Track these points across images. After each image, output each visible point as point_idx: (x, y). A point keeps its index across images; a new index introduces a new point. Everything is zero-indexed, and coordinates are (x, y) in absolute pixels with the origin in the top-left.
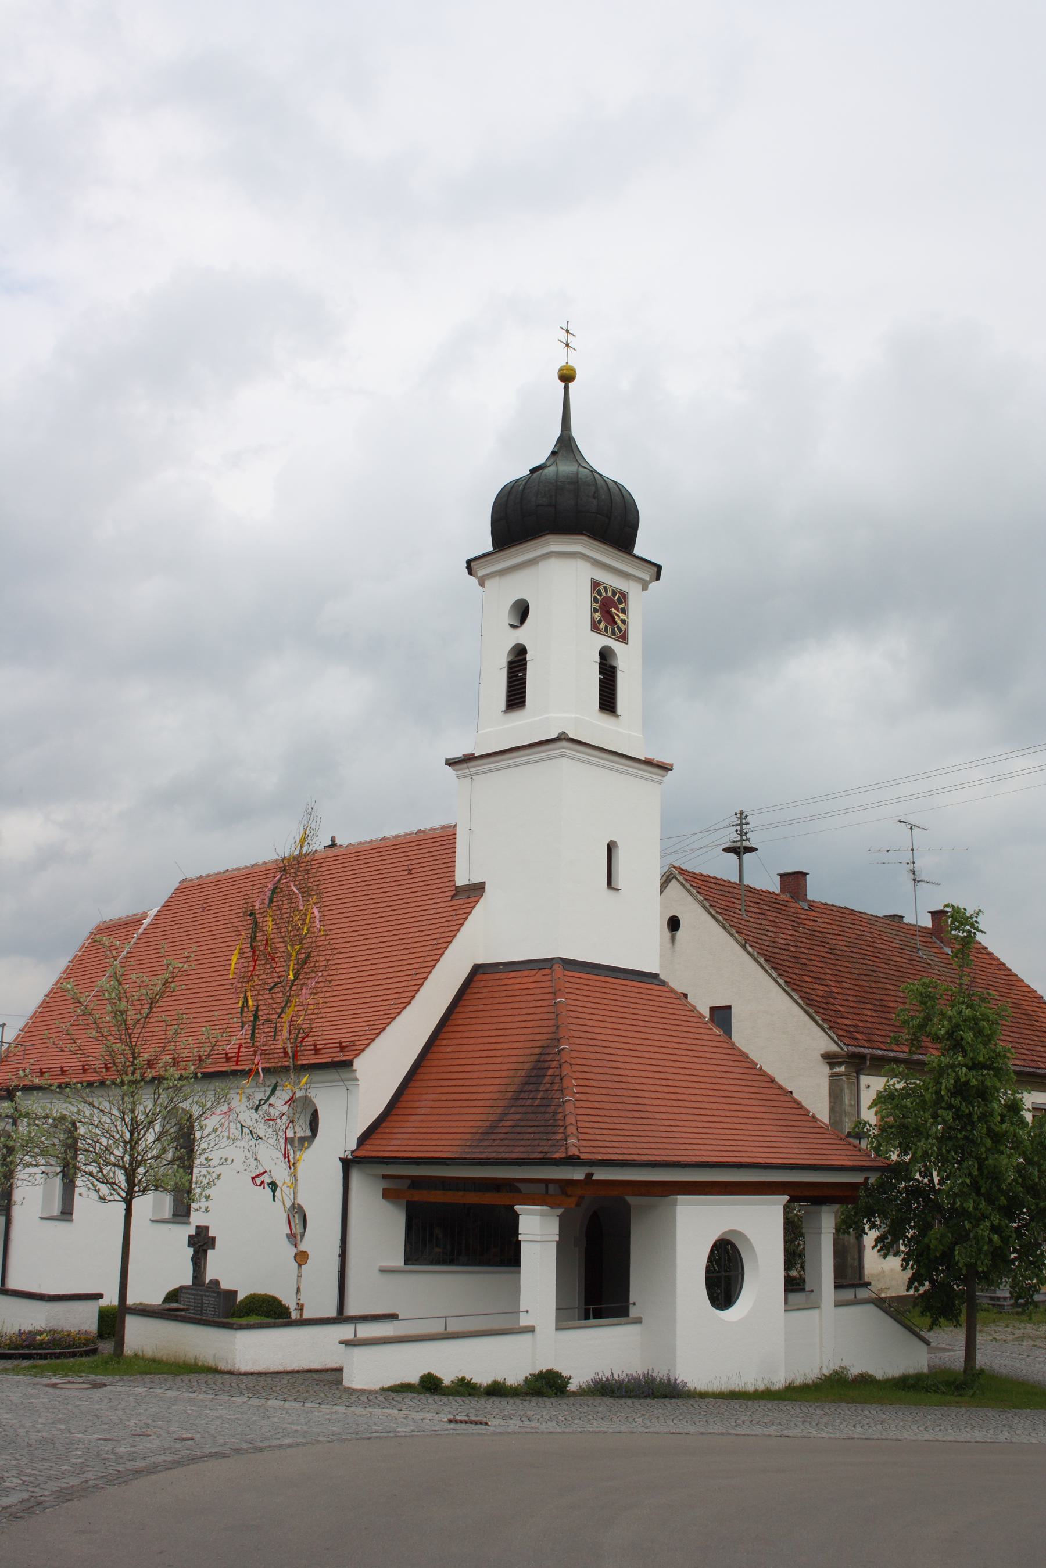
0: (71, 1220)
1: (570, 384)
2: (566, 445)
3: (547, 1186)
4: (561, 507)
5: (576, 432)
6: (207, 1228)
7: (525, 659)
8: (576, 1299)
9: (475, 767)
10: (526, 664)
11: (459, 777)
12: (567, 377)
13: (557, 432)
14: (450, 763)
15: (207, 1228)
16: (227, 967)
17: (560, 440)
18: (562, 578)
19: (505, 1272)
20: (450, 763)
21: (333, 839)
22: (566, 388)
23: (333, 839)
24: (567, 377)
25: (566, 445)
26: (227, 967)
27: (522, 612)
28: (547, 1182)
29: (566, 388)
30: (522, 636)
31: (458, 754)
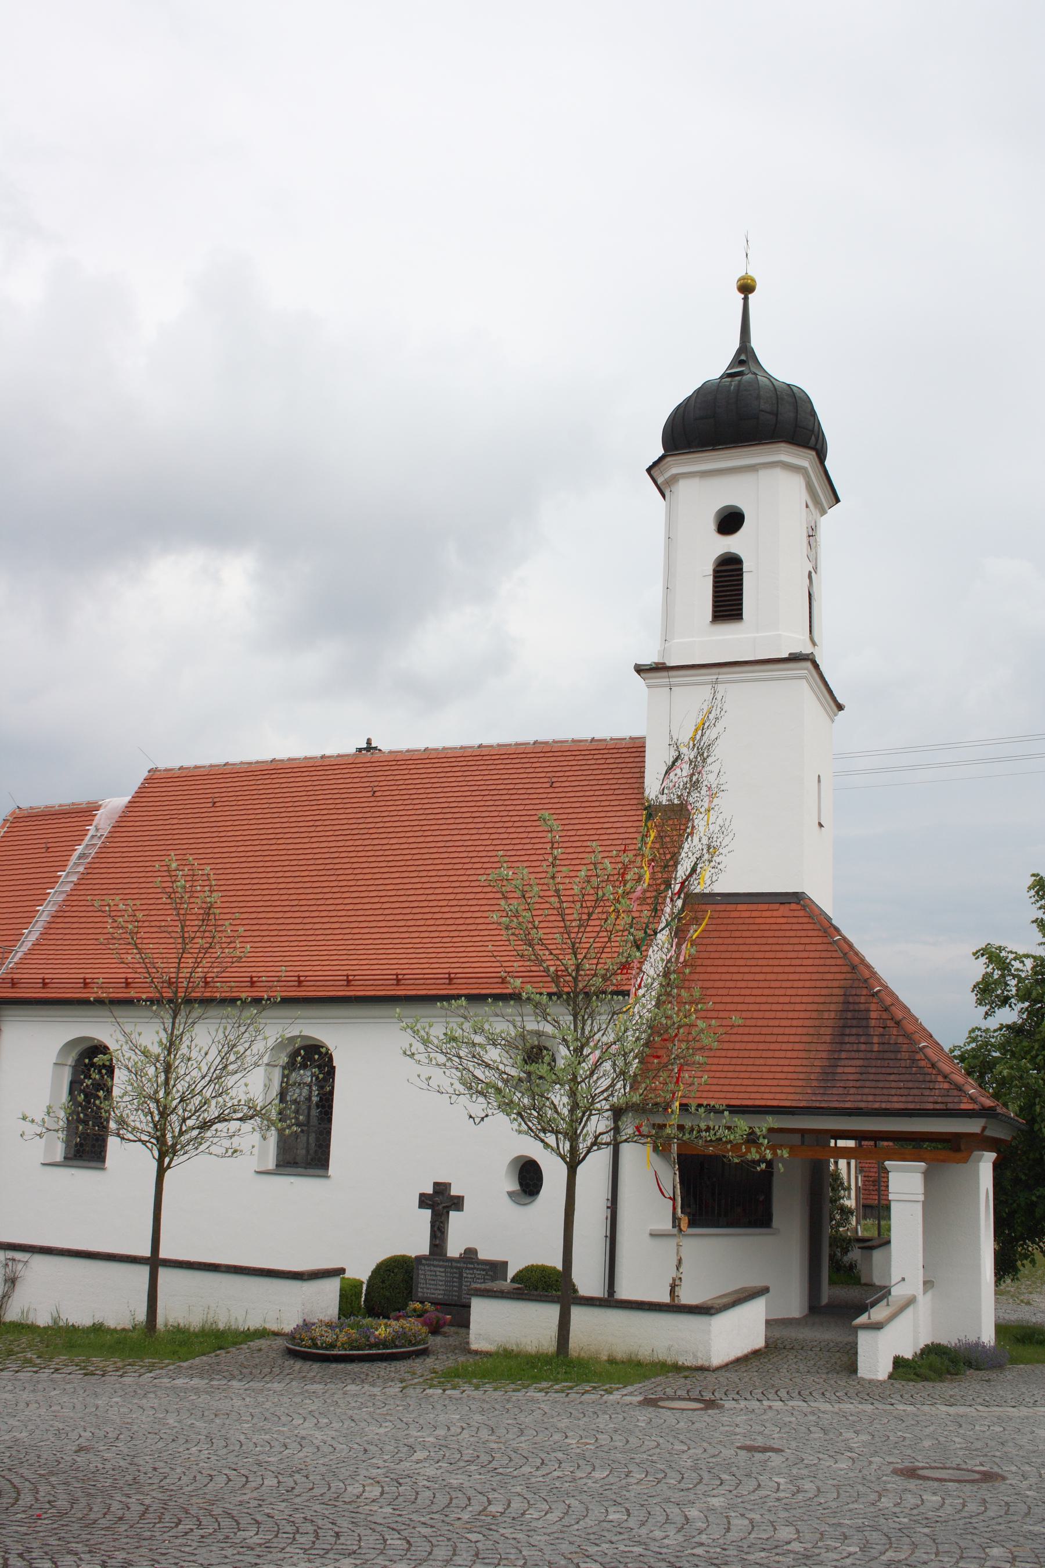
0: (103, 1169)
1: (750, 296)
2: (745, 355)
3: (803, 1136)
4: (741, 417)
5: (755, 343)
6: (422, 1195)
7: (742, 569)
8: (98, 1165)
9: (676, 678)
10: (742, 575)
11: (648, 687)
12: (746, 288)
13: (736, 345)
14: (639, 669)
15: (422, 1195)
16: (716, 915)
17: (739, 352)
18: (767, 485)
19: (760, 1234)
20: (639, 669)
21: (369, 742)
22: (746, 300)
23: (369, 742)
24: (746, 288)
25: (745, 355)
26: (716, 915)
27: (730, 521)
28: (803, 1132)
29: (746, 300)
30: (732, 544)
31: (648, 660)
